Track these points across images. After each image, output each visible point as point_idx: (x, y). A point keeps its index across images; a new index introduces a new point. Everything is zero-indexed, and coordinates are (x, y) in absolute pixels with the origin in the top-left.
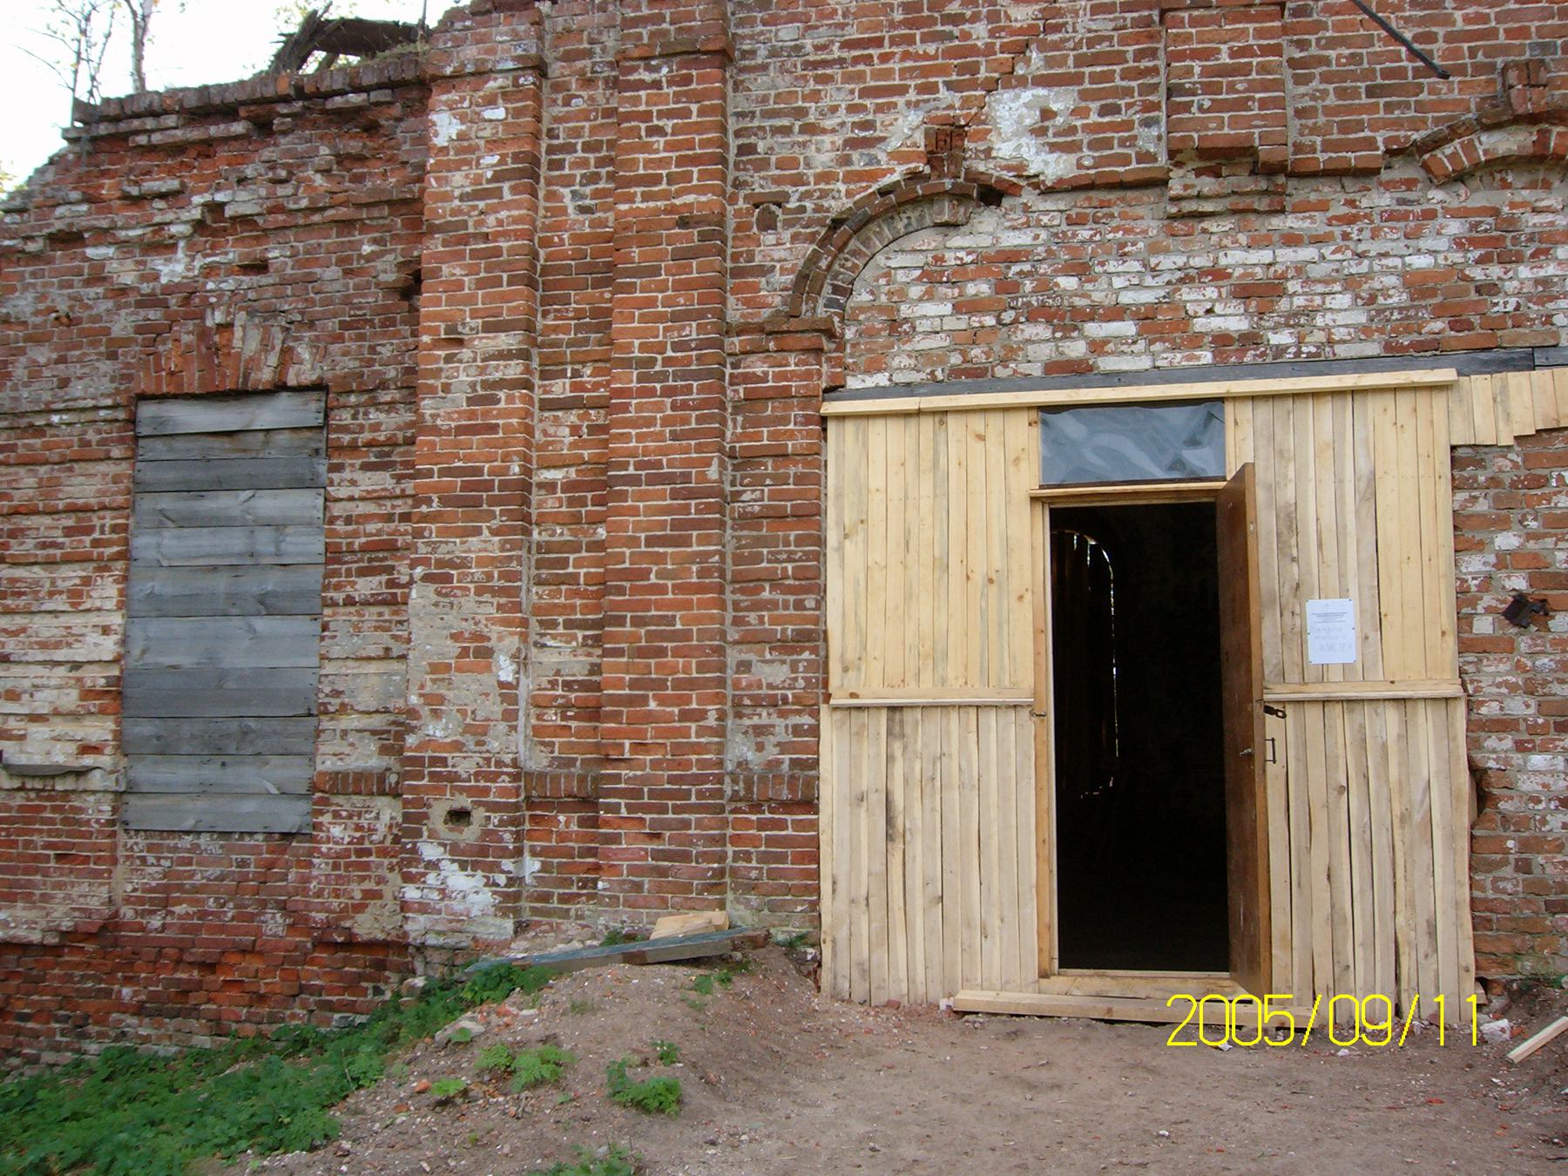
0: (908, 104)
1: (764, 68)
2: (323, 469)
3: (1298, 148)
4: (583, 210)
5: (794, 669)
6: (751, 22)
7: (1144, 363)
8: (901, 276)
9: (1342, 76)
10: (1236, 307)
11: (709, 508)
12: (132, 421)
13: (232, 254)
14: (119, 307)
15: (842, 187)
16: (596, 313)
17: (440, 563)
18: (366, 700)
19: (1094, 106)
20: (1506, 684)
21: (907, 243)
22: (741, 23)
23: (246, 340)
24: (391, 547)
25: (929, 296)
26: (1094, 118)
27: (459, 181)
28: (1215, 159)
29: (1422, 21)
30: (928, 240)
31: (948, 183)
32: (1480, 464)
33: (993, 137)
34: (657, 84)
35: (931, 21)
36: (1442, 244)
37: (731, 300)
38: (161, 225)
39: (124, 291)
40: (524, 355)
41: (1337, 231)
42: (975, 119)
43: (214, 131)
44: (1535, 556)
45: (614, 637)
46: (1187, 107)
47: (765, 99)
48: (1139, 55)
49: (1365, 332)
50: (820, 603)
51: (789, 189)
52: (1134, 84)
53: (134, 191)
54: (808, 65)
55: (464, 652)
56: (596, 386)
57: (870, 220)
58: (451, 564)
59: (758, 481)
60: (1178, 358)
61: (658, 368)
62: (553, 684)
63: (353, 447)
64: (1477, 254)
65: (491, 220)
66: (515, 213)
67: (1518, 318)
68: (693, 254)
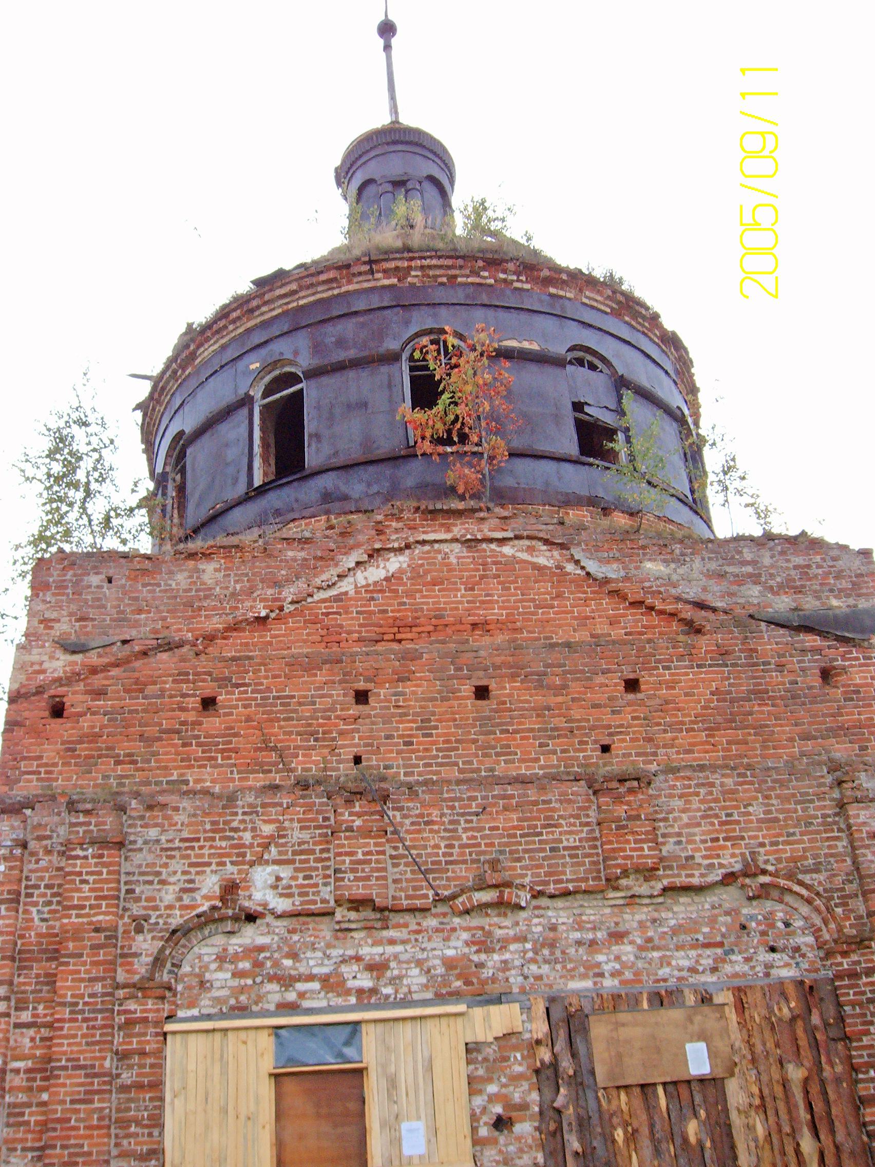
0: (212, 871)
1: (141, 850)
3: (394, 898)
4: (43, 920)
6: (134, 826)
7: (324, 1003)
8: (206, 958)
10: (367, 975)
11: (105, 1083)
15: (178, 912)
16: (47, 975)
19: (301, 875)
20: (495, 1161)
21: (209, 941)
22: (130, 826)
25: (220, 969)
26: (301, 881)
28: (356, 904)
29: (448, 838)
30: (219, 940)
31: (230, 912)
32: (478, 1051)
33: (252, 889)
34: (86, 857)
35: (224, 830)
36: (459, 944)
37: (119, 970)
41: (413, 937)
42: (244, 880)
44: (506, 1096)
45: (50, 1156)
46: (343, 879)
47: (140, 866)
48: (322, 851)
49: (426, 987)
50: (161, 1134)
51: (151, 913)
52: (319, 865)
54: (162, 849)
56: (45, 1015)
57: (190, 930)
59: (130, 1067)
60: (340, 1001)
61: (80, 1007)
64: (474, 948)
66: (7, 922)
67: (494, 979)
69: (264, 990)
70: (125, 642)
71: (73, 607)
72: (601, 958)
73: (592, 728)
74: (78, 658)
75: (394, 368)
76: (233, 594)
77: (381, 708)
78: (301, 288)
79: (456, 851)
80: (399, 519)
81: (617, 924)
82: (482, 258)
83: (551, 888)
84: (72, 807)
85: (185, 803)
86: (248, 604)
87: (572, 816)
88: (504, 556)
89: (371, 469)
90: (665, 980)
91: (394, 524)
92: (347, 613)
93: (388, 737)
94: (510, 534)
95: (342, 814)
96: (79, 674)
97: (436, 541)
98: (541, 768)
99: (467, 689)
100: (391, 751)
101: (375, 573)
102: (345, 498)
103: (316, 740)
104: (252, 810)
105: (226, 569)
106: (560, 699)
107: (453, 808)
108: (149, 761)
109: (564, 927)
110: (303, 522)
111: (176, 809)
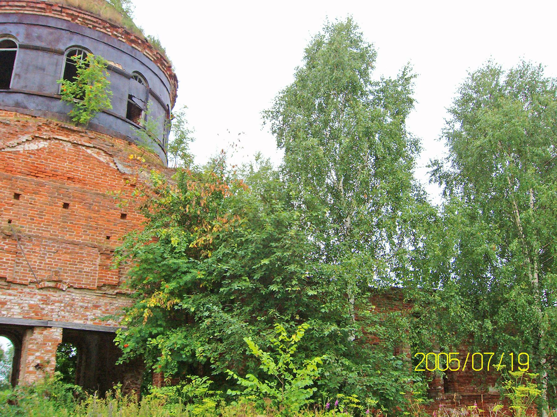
3: (14, 278)
36: (36, 300)
44: (42, 357)
49: (20, 314)
67: (47, 315)
75: (61, 57)
78: (27, 6)
79: (43, 265)
81: (97, 302)
82: (110, 24)
83: (76, 286)
87: (90, 260)
88: (87, 153)
89: (40, 98)
90: (110, 325)
91: (46, 128)
92: (17, 159)
93: (24, 215)
94: (92, 146)
97: (61, 140)
98: (82, 240)
99: (61, 203)
100: (24, 221)
101: (33, 146)
102: (26, 108)
106: (96, 215)
107: (45, 248)
109: (77, 300)
110: (4, 112)
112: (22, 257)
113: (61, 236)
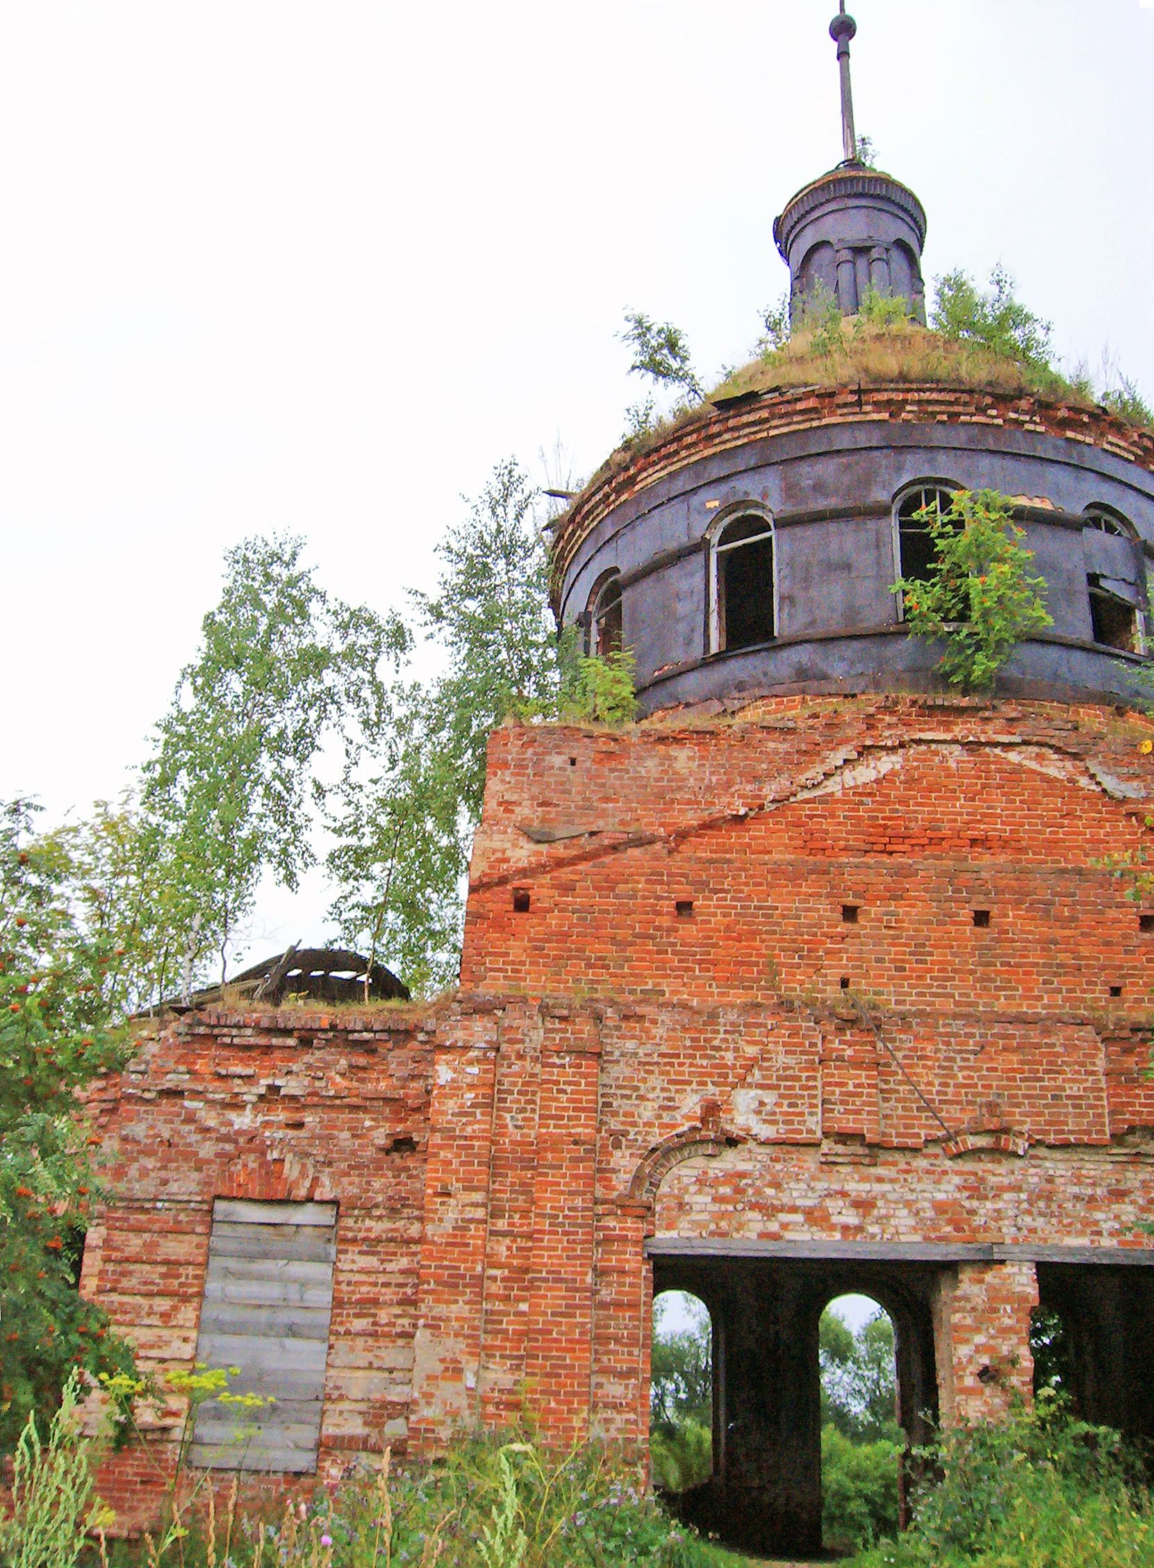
1: (618, 1062)
2: (332, 1249)
3: (884, 1134)
4: (516, 1127)
5: (627, 1386)
8: (685, 1180)
9: (905, 1100)
10: (852, 1211)
11: (586, 1298)
12: (211, 1211)
13: (281, 1116)
14: (205, 1139)
17: (434, 1318)
18: (356, 1393)
19: (786, 1102)
22: (606, 1036)
23: (291, 1170)
24: (375, 1302)
25: (699, 1192)
26: (785, 1108)
27: (451, 1105)
28: (844, 1138)
30: (699, 1162)
34: (563, 1066)
36: (951, 1188)
38: (237, 1094)
39: (208, 1130)
40: (484, 1205)
41: (902, 1177)
43: (274, 1041)
46: (832, 1110)
53: (224, 1072)
54: (640, 1063)
55: (447, 1369)
56: (522, 1225)
58: (440, 1319)
59: (609, 1284)
62: (493, 1390)
63: (354, 1241)
64: (966, 1194)
65: (469, 1129)
67: (986, 1229)
68: (581, 1160)
69: (744, 1218)
70: (592, 834)
71: (535, 790)
72: (1099, 1215)
73: (1103, 968)
74: (543, 848)
75: (883, 523)
76: (709, 788)
77: (872, 928)
78: (773, 417)
79: (950, 1090)
80: (893, 713)
83: (1051, 1138)
84: (545, 1011)
85: (664, 1016)
86: (725, 800)
87: (1076, 1063)
88: (1009, 763)
89: (855, 645)
92: (833, 817)
93: (878, 960)
94: (1017, 739)
95: (832, 1042)
96: (544, 866)
97: (933, 741)
99: (966, 914)
100: (882, 976)
101: (865, 774)
102: (824, 677)
103: (800, 957)
104: (733, 1029)
105: (702, 758)
106: (1067, 932)
108: (622, 967)
110: (773, 700)
111: (654, 1022)
112: (896, 1073)
113: (985, 1005)
